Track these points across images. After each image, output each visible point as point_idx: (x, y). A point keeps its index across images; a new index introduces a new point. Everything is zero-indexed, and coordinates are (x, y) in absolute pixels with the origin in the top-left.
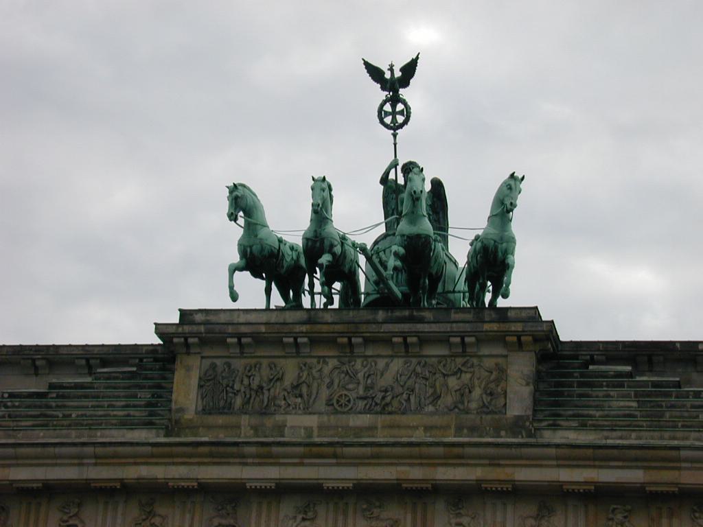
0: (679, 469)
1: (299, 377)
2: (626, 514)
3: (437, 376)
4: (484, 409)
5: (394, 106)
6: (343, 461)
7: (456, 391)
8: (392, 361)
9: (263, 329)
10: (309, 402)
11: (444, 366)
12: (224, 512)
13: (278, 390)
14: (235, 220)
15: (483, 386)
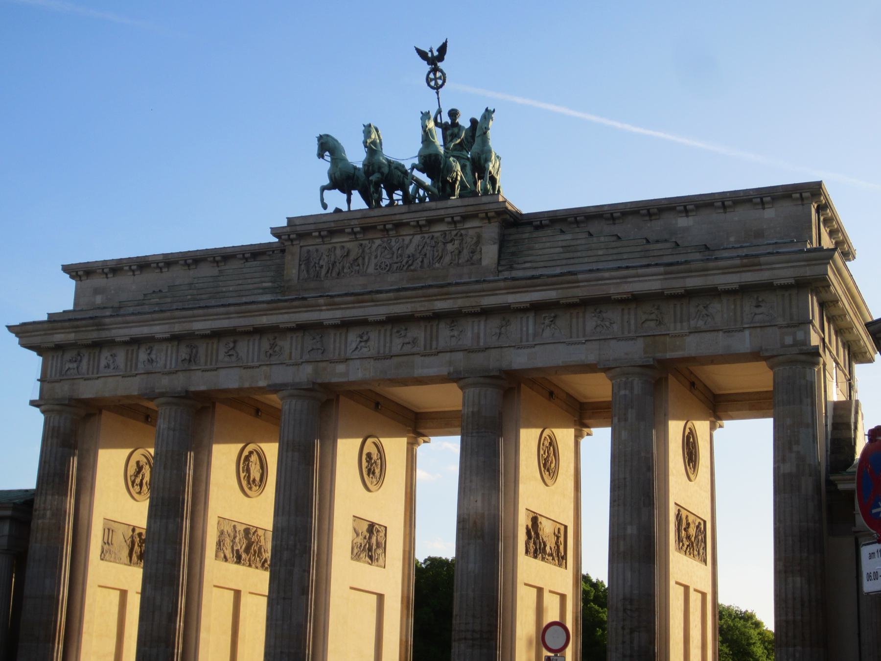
0: (578, 287)
1: (358, 253)
2: (551, 319)
3: (440, 244)
4: (470, 262)
5: (435, 74)
6: (378, 303)
7: (451, 253)
8: (413, 237)
9: (333, 225)
10: (363, 267)
11: (445, 237)
12: (315, 341)
13: (345, 263)
14: (323, 157)
15: (468, 248)
